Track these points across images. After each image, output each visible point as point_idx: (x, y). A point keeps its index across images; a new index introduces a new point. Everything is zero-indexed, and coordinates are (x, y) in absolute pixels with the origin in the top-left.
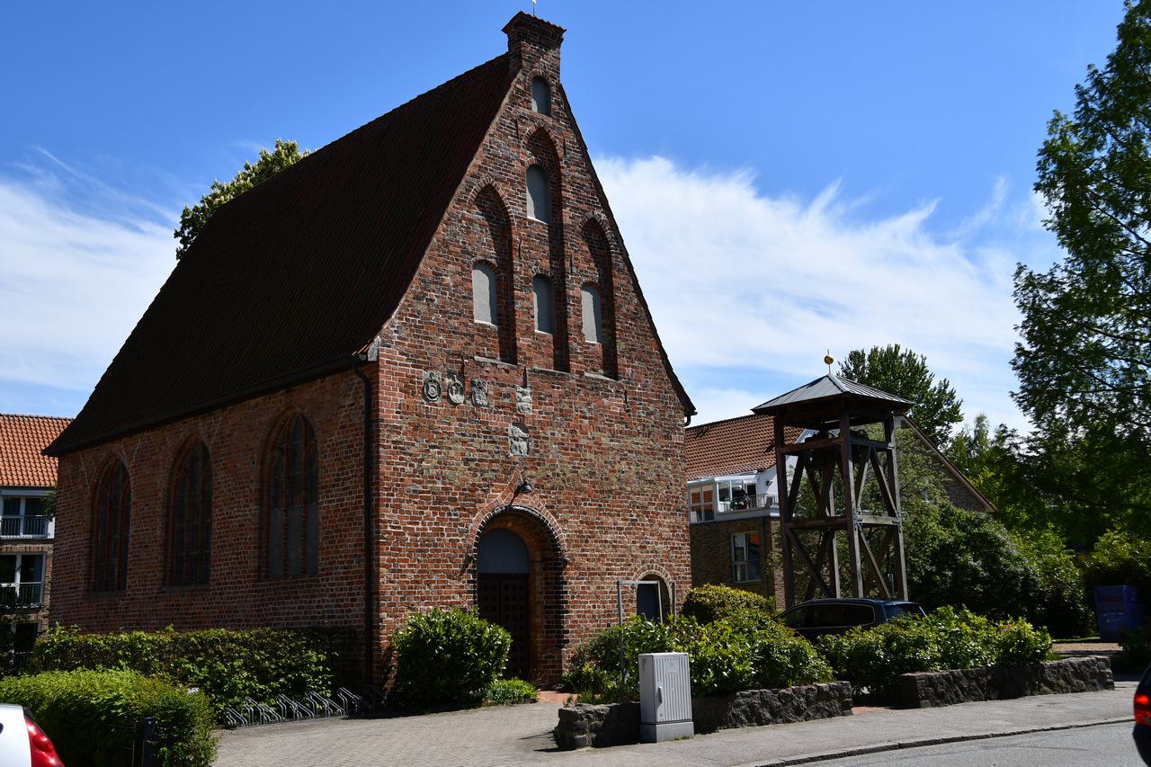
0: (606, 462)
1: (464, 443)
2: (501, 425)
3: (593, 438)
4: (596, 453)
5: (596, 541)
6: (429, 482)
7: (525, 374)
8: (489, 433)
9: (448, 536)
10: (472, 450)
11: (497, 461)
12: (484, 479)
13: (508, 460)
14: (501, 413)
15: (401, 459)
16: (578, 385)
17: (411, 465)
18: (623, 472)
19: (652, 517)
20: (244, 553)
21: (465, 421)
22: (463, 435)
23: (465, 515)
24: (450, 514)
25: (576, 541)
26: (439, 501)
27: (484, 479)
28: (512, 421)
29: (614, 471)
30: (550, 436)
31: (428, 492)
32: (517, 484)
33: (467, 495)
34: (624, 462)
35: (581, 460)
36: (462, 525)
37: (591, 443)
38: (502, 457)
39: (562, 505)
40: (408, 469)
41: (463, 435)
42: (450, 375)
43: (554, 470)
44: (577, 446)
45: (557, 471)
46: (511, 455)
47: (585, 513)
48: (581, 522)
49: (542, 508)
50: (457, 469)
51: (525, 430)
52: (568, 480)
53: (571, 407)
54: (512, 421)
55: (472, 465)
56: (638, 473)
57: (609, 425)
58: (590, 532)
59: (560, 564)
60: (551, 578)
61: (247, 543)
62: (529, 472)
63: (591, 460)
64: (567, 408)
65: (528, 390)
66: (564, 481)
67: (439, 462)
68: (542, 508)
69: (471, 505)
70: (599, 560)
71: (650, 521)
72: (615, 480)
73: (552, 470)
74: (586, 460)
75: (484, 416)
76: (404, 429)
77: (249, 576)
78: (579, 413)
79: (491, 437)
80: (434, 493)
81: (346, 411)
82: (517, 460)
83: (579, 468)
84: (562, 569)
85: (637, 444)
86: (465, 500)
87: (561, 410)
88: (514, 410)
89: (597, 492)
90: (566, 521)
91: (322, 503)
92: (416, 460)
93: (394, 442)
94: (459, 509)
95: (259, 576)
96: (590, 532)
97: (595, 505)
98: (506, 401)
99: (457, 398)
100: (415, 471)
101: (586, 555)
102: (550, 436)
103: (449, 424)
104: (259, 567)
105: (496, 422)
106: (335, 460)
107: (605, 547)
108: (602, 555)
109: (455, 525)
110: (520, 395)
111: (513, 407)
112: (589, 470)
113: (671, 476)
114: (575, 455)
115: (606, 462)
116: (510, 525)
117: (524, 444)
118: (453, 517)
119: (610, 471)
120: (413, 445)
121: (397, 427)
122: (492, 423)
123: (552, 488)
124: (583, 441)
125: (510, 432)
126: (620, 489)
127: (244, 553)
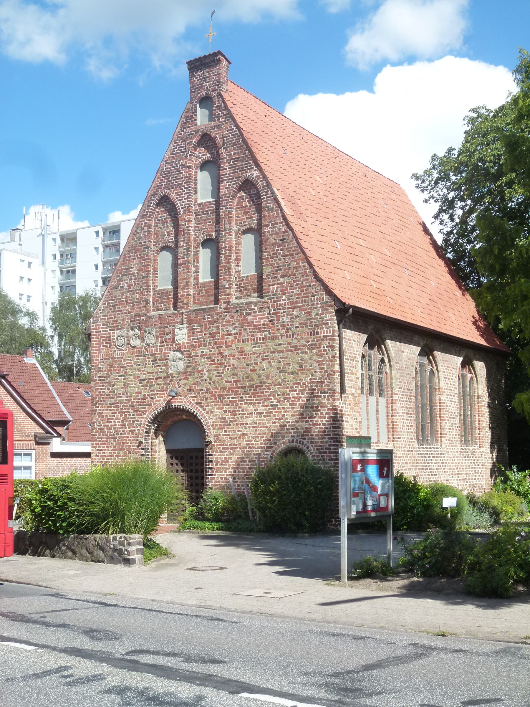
0: (248, 365)
1: (140, 370)
2: (164, 353)
4: (239, 359)
5: (237, 424)
6: (118, 397)
8: (156, 360)
10: (145, 374)
11: (160, 378)
13: (169, 376)
15: (103, 386)
16: (224, 313)
17: (108, 389)
18: (264, 370)
21: (141, 356)
22: (139, 365)
23: (139, 415)
24: (130, 415)
31: (118, 403)
33: (141, 402)
35: (226, 366)
36: (137, 421)
38: (164, 375)
41: (139, 365)
43: (202, 377)
45: (205, 377)
46: (171, 372)
47: (228, 405)
48: (225, 411)
49: (193, 404)
52: (214, 382)
53: (219, 329)
55: (144, 383)
56: (279, 368)
58: (232, 418)
66: (210, 384)
67: (124, 385)
69: (143, 408)
70: (240, 438)
73: (200, 377)
74: (229, 366)
76: (105, 368)
79: (157, 363)
80: (121, 403)
83: (223, 373)
85: (280, 345)
86: (139, 405)
88: (174, 342)
89: (239, 388)
90: (212, 412)
92: (110, 386)
93: (99, 377)
94: (136, 411)
96: (232, 418)
100: (110, 392)
103: (131, 360)
107: (245, 428)
108: (244, 435)
109: (133, 421)
112: (232, 372)
115: (248, 365)
118: (132, 416)
120: (109, 377)
121: (100, 368)
122: (158, 354)
123: (202, 390)
125: (170, 357)
126: (261, 383)
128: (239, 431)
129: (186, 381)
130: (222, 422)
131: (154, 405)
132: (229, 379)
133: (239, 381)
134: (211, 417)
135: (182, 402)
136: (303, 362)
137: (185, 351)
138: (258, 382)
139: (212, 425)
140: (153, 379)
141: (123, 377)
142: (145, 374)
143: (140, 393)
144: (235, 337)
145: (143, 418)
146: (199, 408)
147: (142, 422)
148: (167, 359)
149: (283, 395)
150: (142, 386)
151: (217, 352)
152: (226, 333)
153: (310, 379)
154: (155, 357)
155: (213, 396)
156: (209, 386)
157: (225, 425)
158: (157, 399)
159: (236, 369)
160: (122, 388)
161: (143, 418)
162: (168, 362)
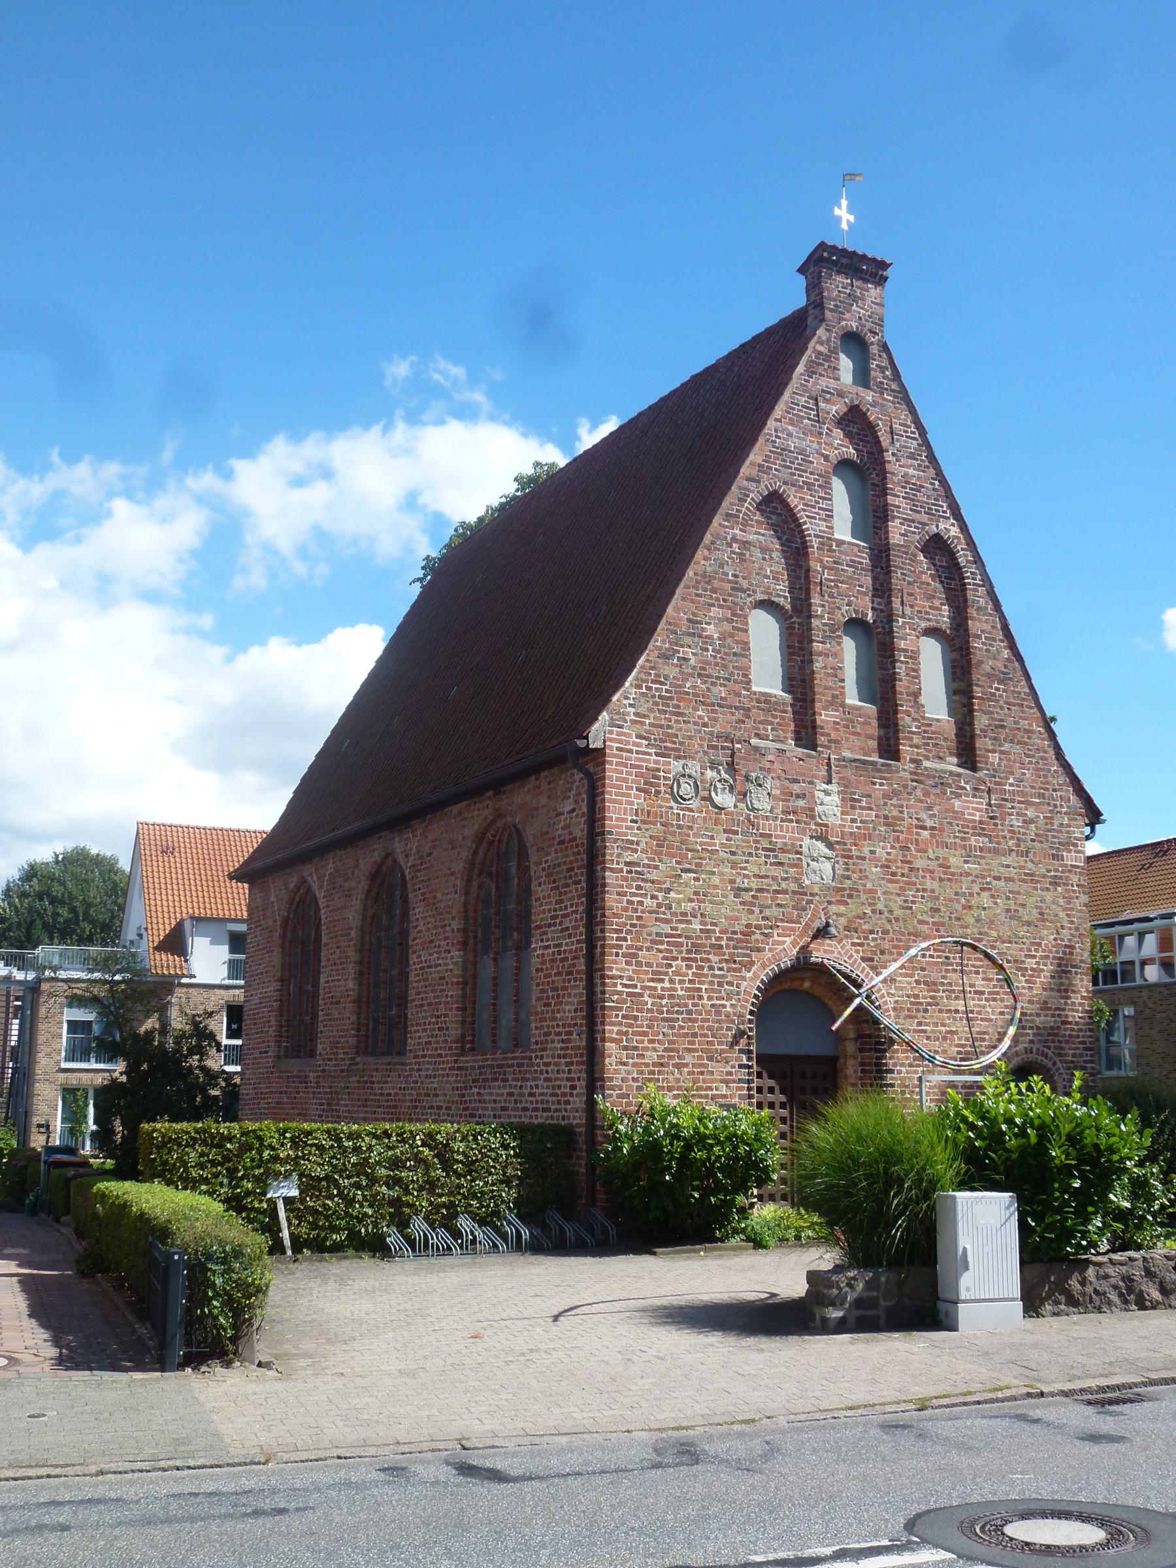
0: (956, 894)
1: (734, 865)
2: (791, 838)
3: (937, 858)
4: (941, 880)
5: (940, 1011)
6: (680, 921)
7: (829, 765)
9: (710, 998)
10: (745, 876)
11: (785, 892)
12: (765, 918)
13: (801, 892)
14: (792, 821)
17: (653, 897)
19: (1030, 976)
20: (446, 1016)
21: (736, 833)
22: (733, 853)
24: (711, 968)
25: (909, 1010)
26: (697, 948)
27: (765, 918)
28: (809, 833)
29: (970, 908)
30: (868, 855)
31: (680, 936)
32: (817, 924)
33: (740, 941)
34: (985, 894)
35: (918, 890)
36: (730, 984)
37: (933, 865)
38: (793, 886)
39: (886, 957)
40: (648, 901)
41: (733, 853)
42: (714, 766)
43: (875, 904)
44: (911, 869)
45: (880, 906)
46: (807, 882)
47: (923, 969)
48: (918, 982)
49: (856, 960)
50: (723, 903)
51: (830, 846)
52: (897, 920)
53: (902, 812)
54: (809, 833)
55: (747, 896)
56: (1008, 911)
57: (963, 839)
58: (931, 997)
59: (883, 1044)
60: (870, 1064)
61: (448, 1003)
62: (834, 909)
63: (933, 891)
64: (895, 813)
65: (834, 788)
66: (889, 921)
68: (856, 960)
69: (745, 955)
71: (1027, 981)
72: (972, 921)
73: (870, 904)
74: (924, 890)
75: (765, 826)
76: (643, 845)
77: (450, 1048)
78: (915, 822)
79: (776, 857)
80: (687, 937)
81: (565, 819)
82: (816, 890)
83: (913, 902)
84: (885, 1051)
85: (1008, 866)
86: (735, 948)
87: (886, 817)
88: (813, 817)
91: (535, 949)
92: (660, 890)
94: (727, 961)
95: (463, 1049)
96: (931, 997)
97: (939, 957)
98: (801, 803)
99: (725, 799)
100: (659, 905)
101: (924, 1031)
102: (868, 855)
104: (463, 1036)
105: (784, 833)
106: (552, 889)
107: (955, 1019)
109: (720, 984)
110: (821, 795)
111: (810, 813)
112: (930, 905)
113: (1062, 914)
114: (907, 883)
115: (956, 894)
116: (807, 984)
117: (827, 867)
118: (717, 972)
119: (964, 907)
120: (656, 867)
121: (632, 842)
122: (777, 837)
123: (872, 932)
124: (920, 863)
125: (805, 850)
126: (980, 933)
127: (446, 1016)
128: (943, 1025)
129: (842, 908)
130: (912, 1003)
131: (770, 950)
132: (925, 917)
133: (943, 924)
134: (892, 991)
135: (833, 952)
136: (1044, 906)
137: (838, 843)
138: (975, 930)
139: (895, 1009)
140: (768, 891)
141: (692, 875)
142: (745, 876)
143: (737, 919)
144: (932, 835)
145: (743, 978)
146: (868, 969)
147: (743, 989)
148: (800, 853)
149: (1016, 961)
150: (742, 903)
151: (900, 858)
152: (915, 822)
153: (1055, 939)
154: (771, 843)
155: (895, 947)
156: (888, 927)
157: (918, 1010)
158: (776, 938)
159: (937, 898)
160: (691, 900)
161: (743, 978)
162: (800, 859)
